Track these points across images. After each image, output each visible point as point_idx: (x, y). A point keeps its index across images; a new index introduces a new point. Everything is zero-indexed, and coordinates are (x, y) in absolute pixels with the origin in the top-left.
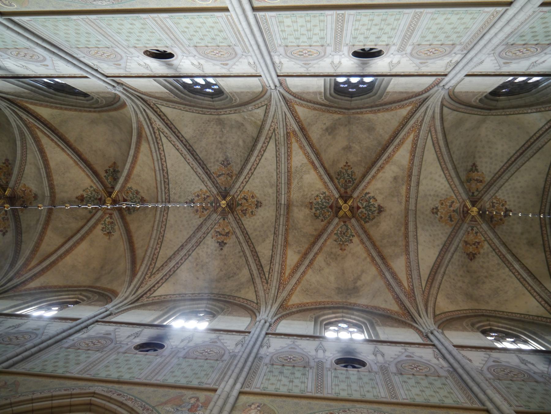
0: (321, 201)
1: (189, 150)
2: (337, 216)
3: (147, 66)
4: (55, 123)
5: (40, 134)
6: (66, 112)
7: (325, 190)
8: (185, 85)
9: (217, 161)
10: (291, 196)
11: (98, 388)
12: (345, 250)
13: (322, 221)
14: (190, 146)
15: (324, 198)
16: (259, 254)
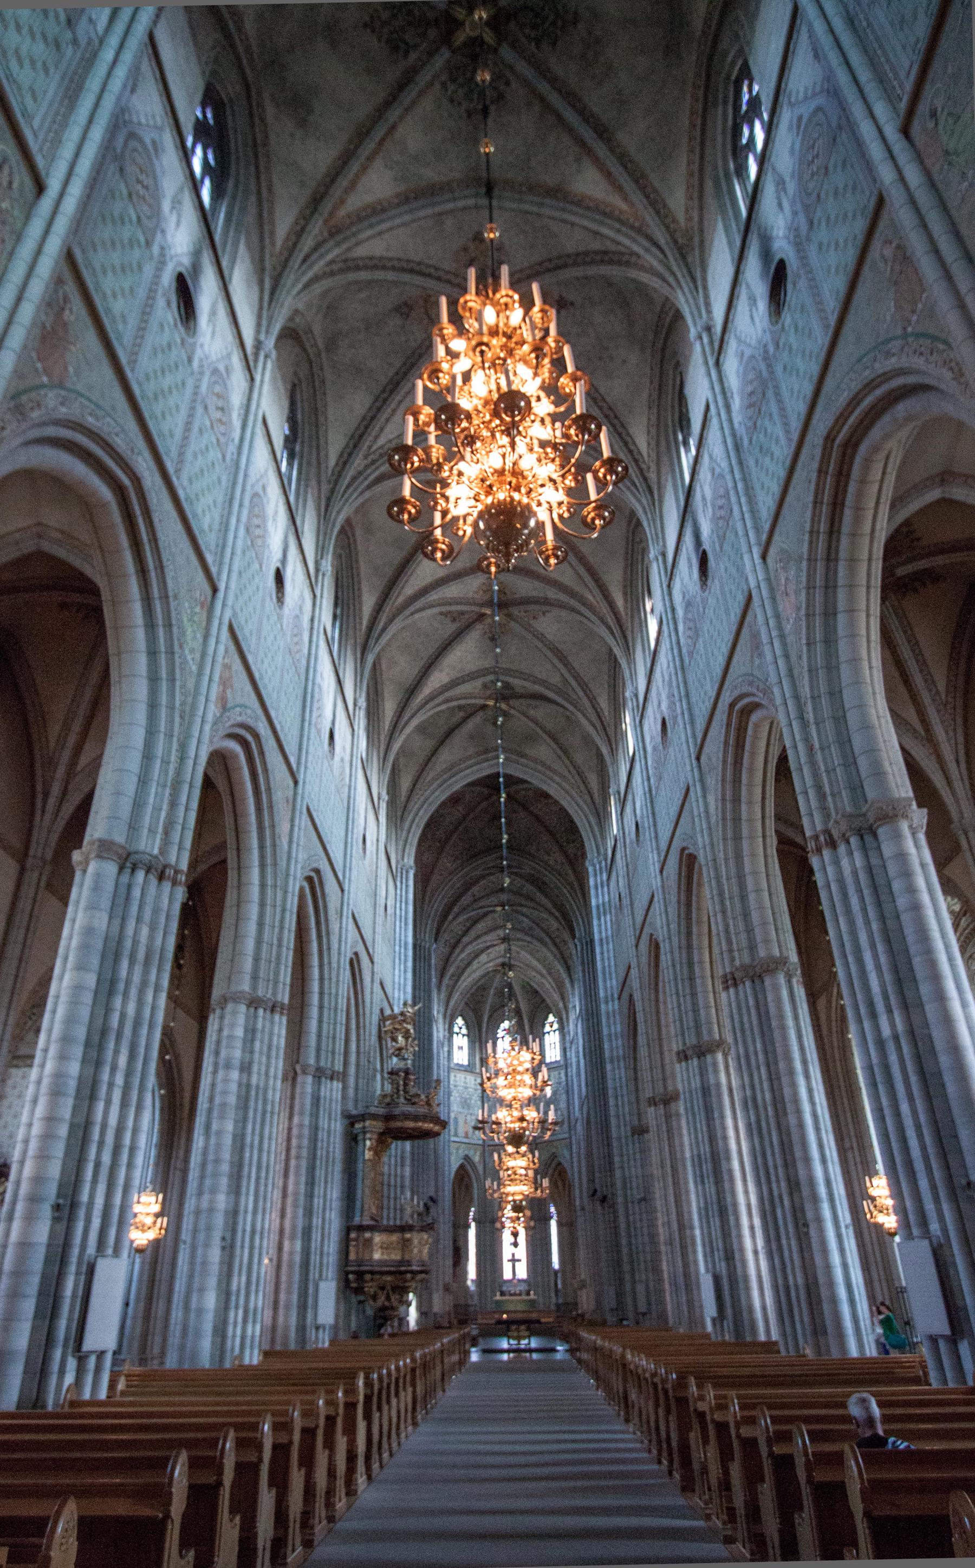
0: (462, 86)
1: (392, 392)
2: (496, 51)
3: (213, 313)
4: (380, 584)
5: (401, 599)
6: (362, 574)
7: (437, 86)
8: (217, 193)
9: (403, 327)
10: (457, 175)
11: (726, 698)
12: (576, 13)
13: (508, 83)
14: (384, 391)
15: (454, 80)
16: (581, 249)
